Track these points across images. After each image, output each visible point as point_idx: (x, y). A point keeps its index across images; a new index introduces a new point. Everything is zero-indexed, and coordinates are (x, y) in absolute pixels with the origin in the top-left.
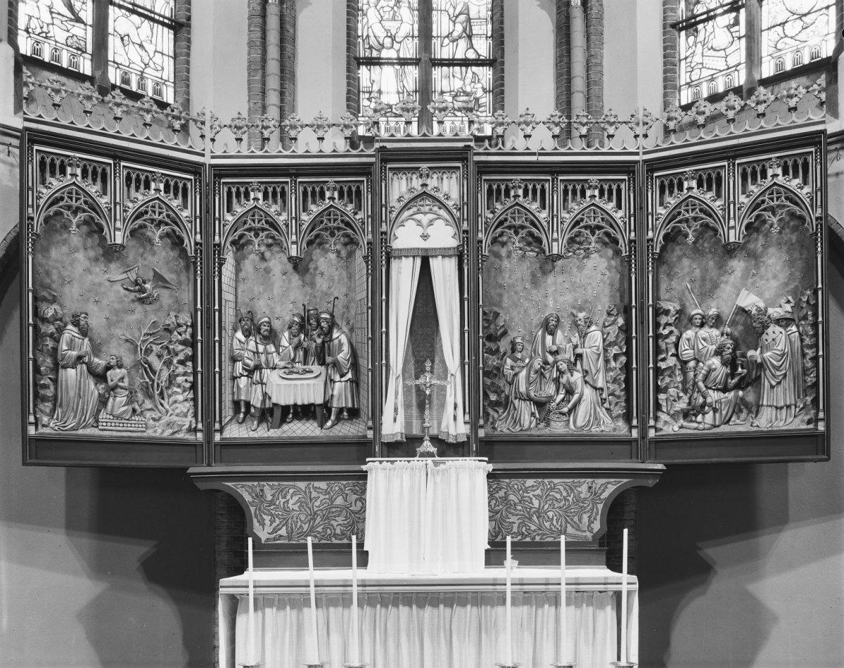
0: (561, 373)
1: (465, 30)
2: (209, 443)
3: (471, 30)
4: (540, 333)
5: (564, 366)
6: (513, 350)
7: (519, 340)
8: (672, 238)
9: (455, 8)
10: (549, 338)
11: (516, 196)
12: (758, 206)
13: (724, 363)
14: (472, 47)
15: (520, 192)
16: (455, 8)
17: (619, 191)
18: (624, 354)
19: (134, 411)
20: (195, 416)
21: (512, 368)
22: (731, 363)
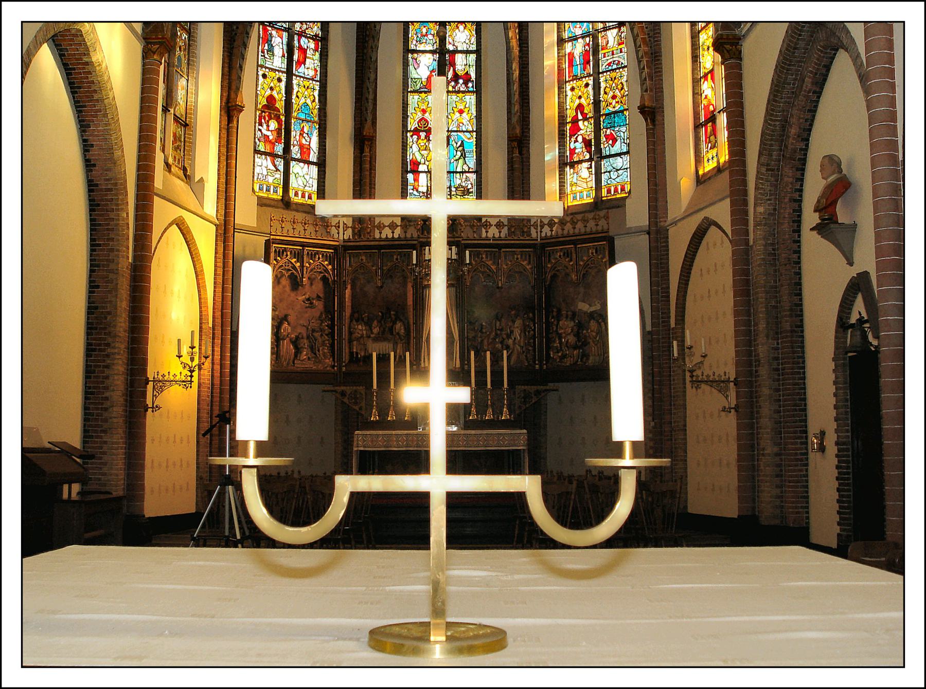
0: (504, 339)
1: (462, 155)
2: (340, 372)
3: (465, 155)
4: (494, 321)
5: (505, 336)
6: (482, 328)
7: (484, 324)
8: (554, 277)
9: (457, 144)
10: (498, 323)
11: (482, 258)
12: (587, 266)
13: (574, 335)
14: (466, 163)
15: (484, 256)
16: (457, 144)
17: (530, 256)
18: (532, 330)
19: (309, 358)
20: (334, 360)
21: (481, 337)
22: (577, 335)
